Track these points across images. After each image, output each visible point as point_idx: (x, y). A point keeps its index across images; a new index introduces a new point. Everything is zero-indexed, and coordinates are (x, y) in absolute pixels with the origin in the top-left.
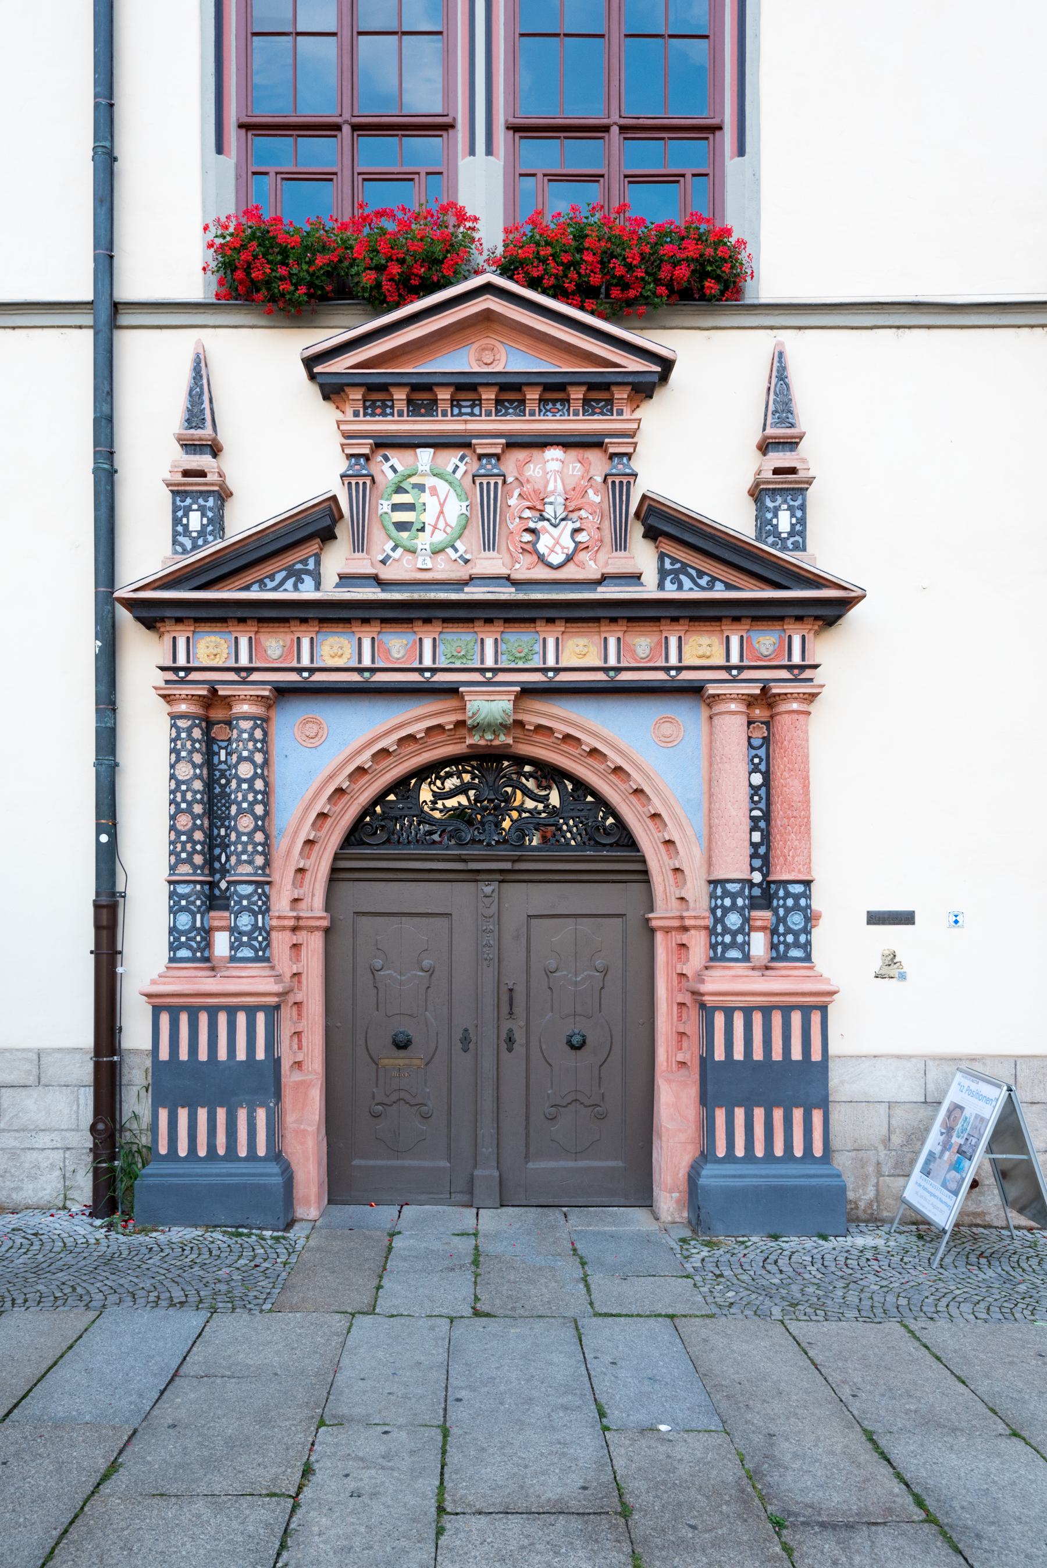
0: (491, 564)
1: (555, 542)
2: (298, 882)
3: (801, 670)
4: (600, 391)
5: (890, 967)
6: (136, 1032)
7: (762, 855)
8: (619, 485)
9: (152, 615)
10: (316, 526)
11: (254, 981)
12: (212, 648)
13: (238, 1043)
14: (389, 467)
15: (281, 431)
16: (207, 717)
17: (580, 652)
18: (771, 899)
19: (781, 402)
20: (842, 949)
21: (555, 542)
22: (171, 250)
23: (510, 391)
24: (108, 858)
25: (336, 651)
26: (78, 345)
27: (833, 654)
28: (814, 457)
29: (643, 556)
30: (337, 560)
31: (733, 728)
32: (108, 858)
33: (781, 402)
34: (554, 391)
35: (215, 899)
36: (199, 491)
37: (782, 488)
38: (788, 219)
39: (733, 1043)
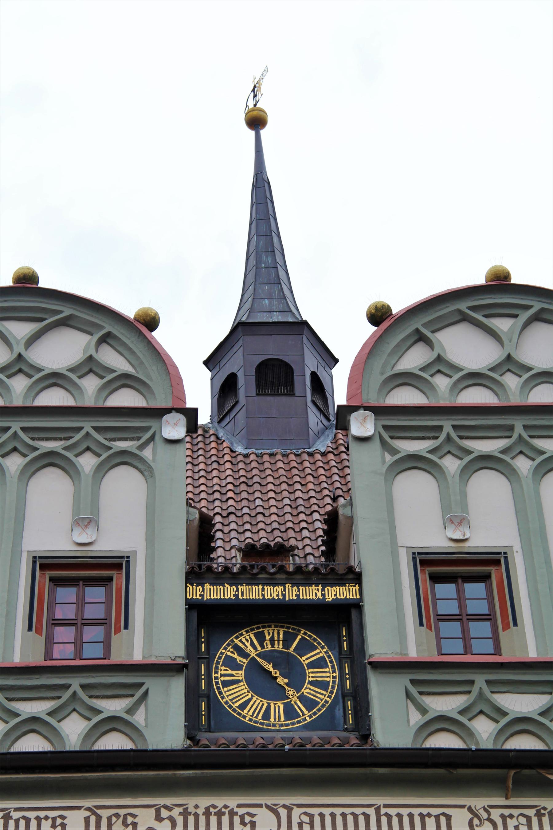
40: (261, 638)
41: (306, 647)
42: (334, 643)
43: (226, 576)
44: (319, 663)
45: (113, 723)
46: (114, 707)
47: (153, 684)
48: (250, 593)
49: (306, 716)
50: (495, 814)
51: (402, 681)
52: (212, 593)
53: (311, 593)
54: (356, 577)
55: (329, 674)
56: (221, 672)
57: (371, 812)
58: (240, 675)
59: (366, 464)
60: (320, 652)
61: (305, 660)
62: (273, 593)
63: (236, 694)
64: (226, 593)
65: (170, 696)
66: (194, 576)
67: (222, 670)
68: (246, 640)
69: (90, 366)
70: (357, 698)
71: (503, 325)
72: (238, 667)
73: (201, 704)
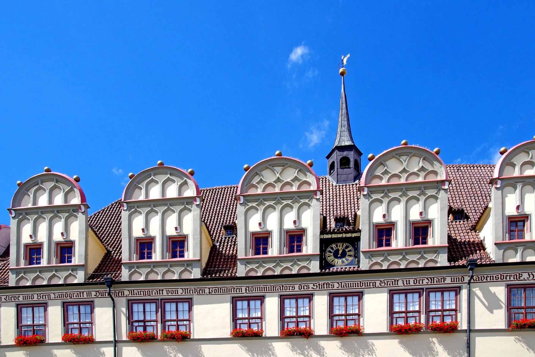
40: (337, 246)
41: (347, 247)
43: (330, 233)
44: (350, 251)
48: (334, 236)
50: (386, 282)
52: (326, 236)
53: (349, 235)
54: (360, 231)
56: (328, 254)
57: (359, 282)
58: (332, 254)
60: (350, 248)
61: (347, 250)
62: (340, 236)
64: (329, 236)
66: (322, 233)
67: (328, 253)
68: (334, 246)
72: (331, 252)
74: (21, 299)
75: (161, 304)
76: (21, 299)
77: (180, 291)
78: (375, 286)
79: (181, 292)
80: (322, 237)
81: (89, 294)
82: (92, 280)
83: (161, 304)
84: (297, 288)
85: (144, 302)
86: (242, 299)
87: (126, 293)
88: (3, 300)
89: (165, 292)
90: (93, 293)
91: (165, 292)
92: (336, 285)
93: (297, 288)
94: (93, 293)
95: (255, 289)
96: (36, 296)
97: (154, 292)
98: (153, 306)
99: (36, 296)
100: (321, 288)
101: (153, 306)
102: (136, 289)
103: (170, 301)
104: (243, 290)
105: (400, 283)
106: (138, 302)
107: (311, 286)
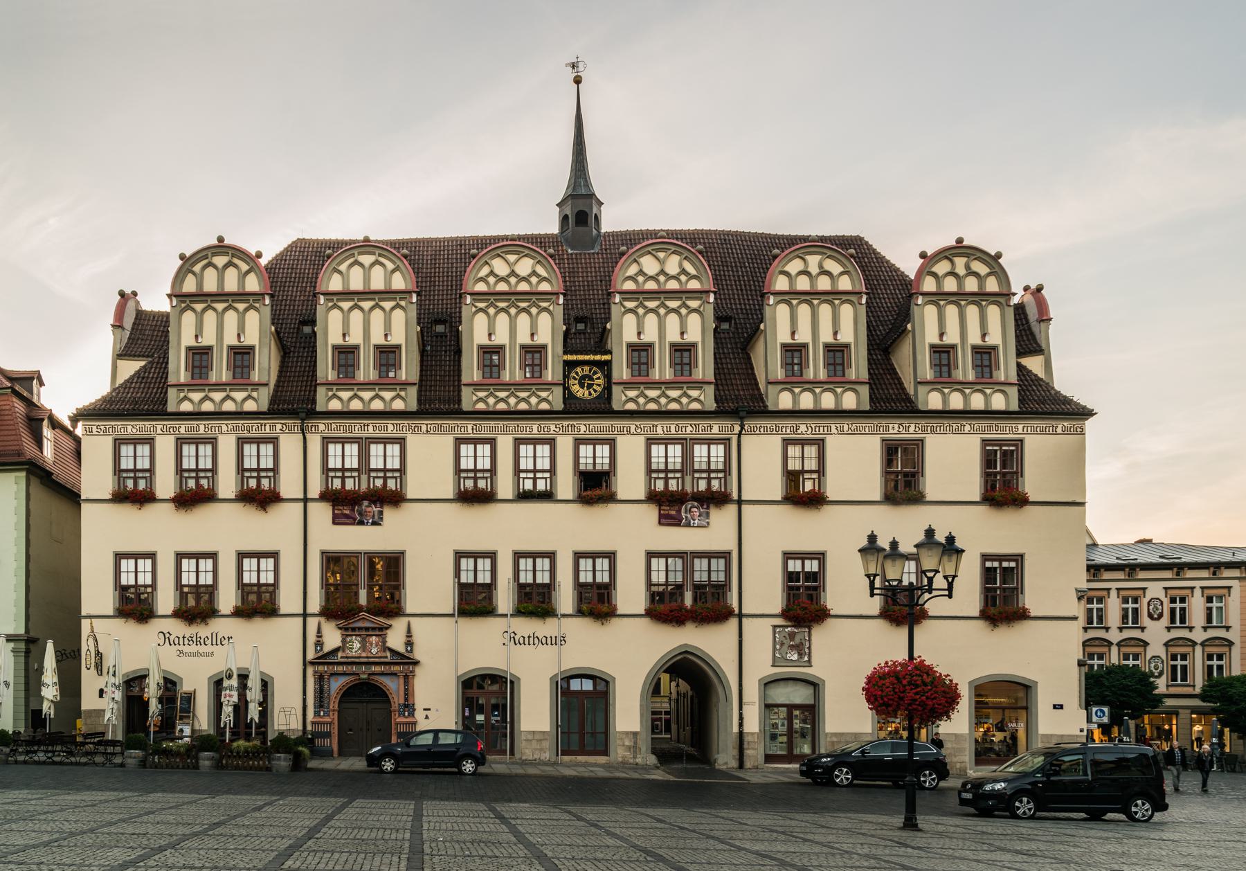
0: (364, 655)
1: (374, 651)
2: (334, 705)
3: (413, 672)
4: (381, 629)
5: (427, 717)
6: (309, 728)
7: (406, 700)
8: (384, 642)
9: (312, 663)
10: (336, 650)
11: (327, 719)
12: (321, 668)
13: (325, 729)
14: (349, 639)
15: (332, 637)
16: (320, 678)
17: (377, 669)
18: (409, 707)
19: (409, 630)
20: (419, 715)
21: (374, 651)
22: (315, 605)
23: (367, 629)
24: (304, 700)
25: (340, 669)
26: (301, 619)
27: (418, 670)
28: (415, 639)
29: (388, 654)
30: (340, 654)
31: (402, 680)
32: (304, 700)
33: (409, 630)
34: (374, 629)
35: (321, 706)
36: (319, 644)
37: (409, 644)
38: (410, 606)
39: (402, 729)
41: (595, 373)
42: (603, 372)
45: (545, 400)
46: (544, 394)
47: (554, 388)
48: (580, 357)
49: (594, 395)
51: (621, 387)
55: (601, 382)
56: (572, 381)
59: (615, 310)
62: (587, 358)
63: (575, 388)
64: (574, 357)
65: (558, 391)
68: (579, 370)
69: (534, 273)
70: (608, 388)
71: (661, 255)
73: (568, 396)
74: (182, 430)
75: (364, 445)
76: (182, 430)
77: (390, 427)
78: (629, 433)
79: (391, 428)
80: (565, 358)
81: (273, 427)
82: (277, 409)
83: (364, 445)
84: (535, 431)
85: (343, 441)
86: (467, 441)
87: (322, 427)
88: (159, 431)
89: (371, 428)
90: (279, 427)
91: (371, 430)
92: (583, 428)
93: (535, 431)
94: (279, 427)
95: (485, 428)
96: (202, 427)
97: (358, 428)
98: (355, 447)
99: (202, 427)
100: (565, 431)
101: (355, 447)
102: (335, 423)
103: (377, 440)
104: (469, 428)
105: (659, 430)
106: (335, 440)
107: (553, 427)
